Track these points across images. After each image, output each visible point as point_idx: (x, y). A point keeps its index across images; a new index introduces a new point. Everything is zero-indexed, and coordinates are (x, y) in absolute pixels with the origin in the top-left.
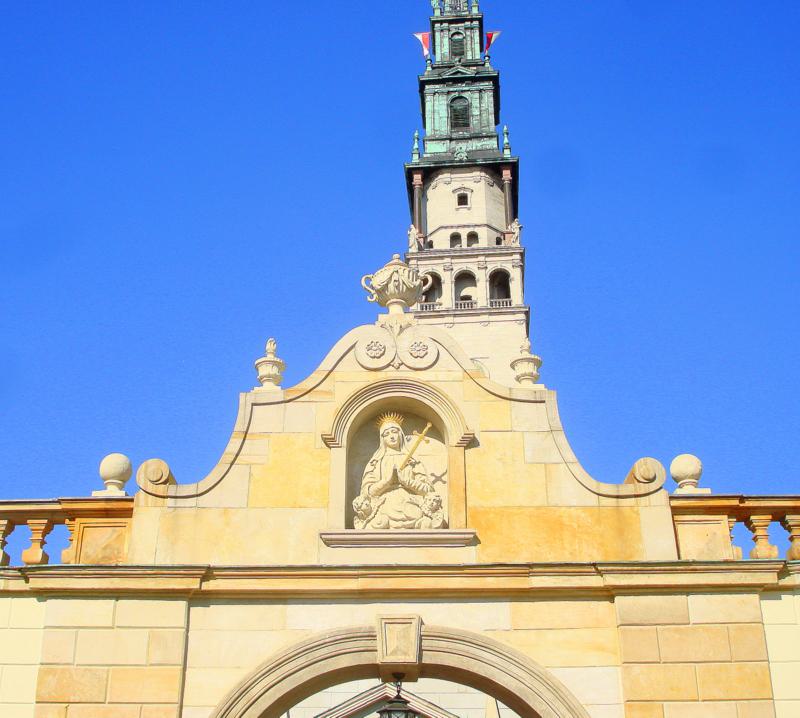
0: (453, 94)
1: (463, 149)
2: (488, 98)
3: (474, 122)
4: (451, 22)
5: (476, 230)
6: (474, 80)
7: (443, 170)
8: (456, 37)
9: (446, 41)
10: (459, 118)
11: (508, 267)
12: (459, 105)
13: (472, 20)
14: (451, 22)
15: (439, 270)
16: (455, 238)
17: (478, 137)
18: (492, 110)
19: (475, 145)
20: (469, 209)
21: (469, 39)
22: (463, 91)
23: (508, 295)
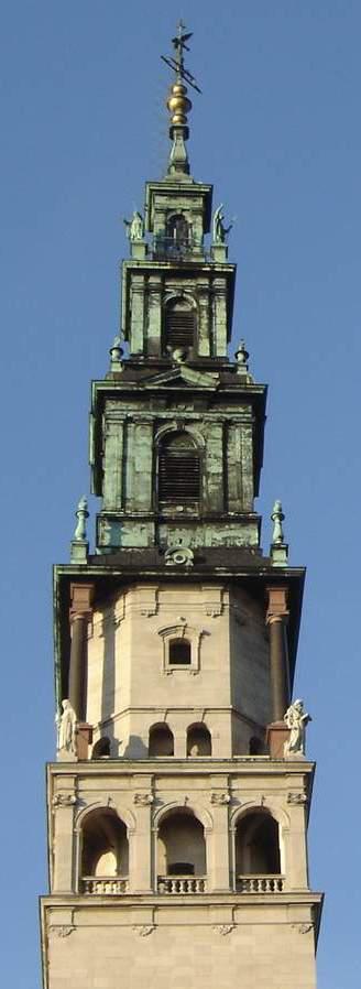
0: (166, 427)
1: (183, 545)
2: (241, 441)
3: (211, 487)
6: (210, 400)
9: (156, 313)
17: (218, 519)
18: (247, 463)
19: (211, 536)
23: (273, 865)
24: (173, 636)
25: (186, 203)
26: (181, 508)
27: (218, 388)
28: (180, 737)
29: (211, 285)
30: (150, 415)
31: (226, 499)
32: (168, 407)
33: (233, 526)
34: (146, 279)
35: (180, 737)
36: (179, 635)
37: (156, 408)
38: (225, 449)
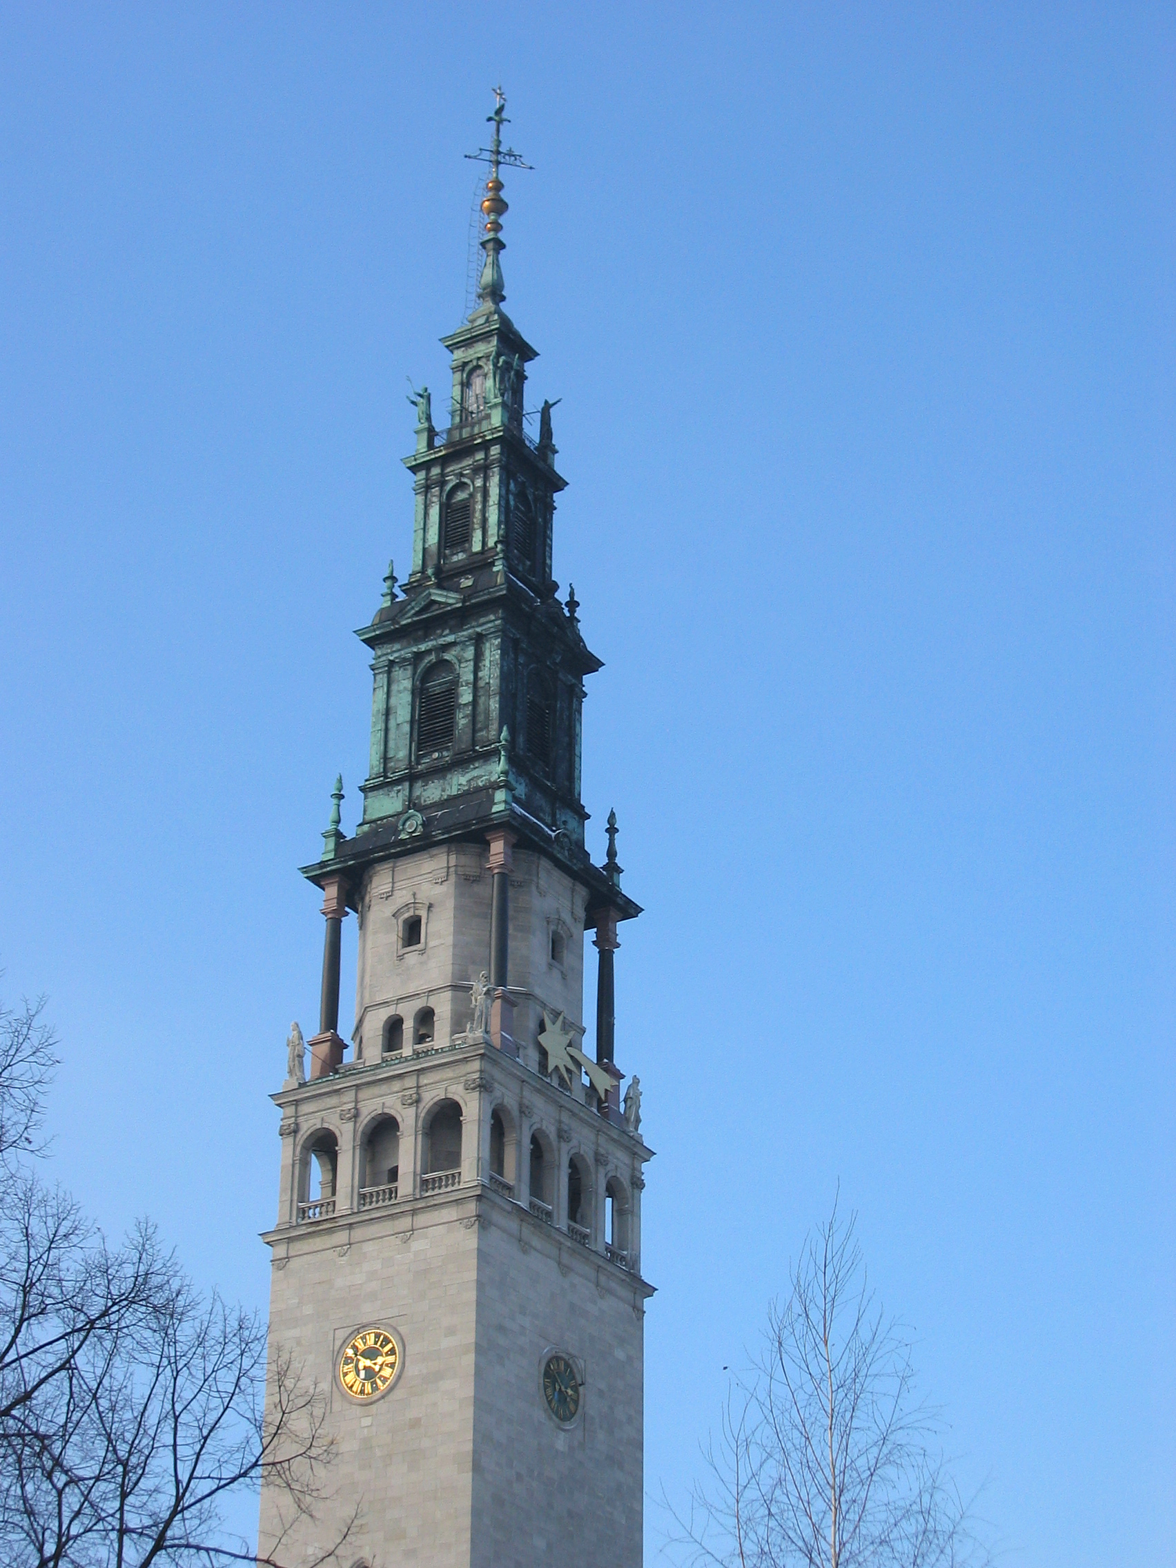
2: (492, 653)
3: (462, 720)
4: (444, 461)
5: (433, 1002)
7: (378, 867)
8: (461, 496)
9: (435, 512)
10: (433, 718)
11: (456, 1092)
12: (436, 685)
13: (486, 446)
14: (444, 461)
16: (393, 1028)
17: (462, 762)
19: (458, 782)
21: (479, 497)
22: (446, 647)
24: (406, 915)
25: (481, 349)
26: (436, 755)
27: (464, 601)
28: (408, 1026)
29: (486, 459)
30: (407, 653)
31: (474, 731)
32: (425, 638)
35: (408, 1026)
37: (418, 641)
38: (476, 669)
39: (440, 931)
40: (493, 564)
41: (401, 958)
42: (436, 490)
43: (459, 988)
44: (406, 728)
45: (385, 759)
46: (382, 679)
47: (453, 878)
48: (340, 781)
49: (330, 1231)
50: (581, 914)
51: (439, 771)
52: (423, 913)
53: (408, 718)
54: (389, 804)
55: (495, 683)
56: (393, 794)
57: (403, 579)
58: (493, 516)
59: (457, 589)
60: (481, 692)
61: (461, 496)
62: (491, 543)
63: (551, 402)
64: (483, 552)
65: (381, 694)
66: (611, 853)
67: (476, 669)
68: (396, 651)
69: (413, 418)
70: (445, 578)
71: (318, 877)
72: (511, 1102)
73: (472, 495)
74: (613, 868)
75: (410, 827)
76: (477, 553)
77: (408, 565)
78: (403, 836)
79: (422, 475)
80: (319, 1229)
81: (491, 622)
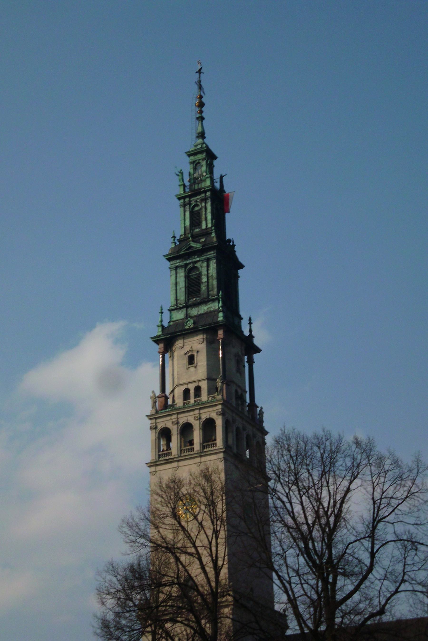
2: (213, 265)
3: (203, 288)
4: (190, 196)
8: (197, 209)
9: (188, 214)
10: (193, 286)
11: (213, 415)
12: (193, 274)
13: (205, 192)
14: (190, 196)
15: (169, 425)
16: (186, 392)
17: (205, 302)
19: (204, 309)
20: (196, 367)
21: (204, 210)
25: (200, 156)
26: (195, 299)
27: (203, 246)
28: (192, 392)
31: (208, 291)
33: (210, 303)
34: (184, 200)
35: (192, 392)
36: (190, 354)
37: (186, 260)
38: (208, 270)
39: (202, 360)
40: (211, 233)
41: (188, 368)
42: (188, 206)
43: (210, 379)
44: (183, 289)
45: (177, 300)
46: (174, 272)
47: (205, 343)
48: (162, 307)
49: (171, 462)
50: (244, 352)
51: (196, 305)
52: (195, 354)
53: (184, 286)
54: (179, 315)
55: (215, 275)
56: (180, 312)
57: (178, 238)
58: (209, 217)
59: (199, 243)
60: (210, 278)
61: (197, 209)
62: (209, 225)
63: (223, 175)
64: (206, 228)
65: (174, 277)
66: (251, 331)
67: (208, 270)
68: (178, 262)
69: (177, 181)
70: (196, 238)
71: (157, 340)
72: (230, 419)
73: (201, 209)
74: (251, 337)
75: (189, 324)
76: (204, 229)
77: (180, 232)
78: (187, 327)
79: (182, 201)
80: (168, 462)
81: (212, 254)
